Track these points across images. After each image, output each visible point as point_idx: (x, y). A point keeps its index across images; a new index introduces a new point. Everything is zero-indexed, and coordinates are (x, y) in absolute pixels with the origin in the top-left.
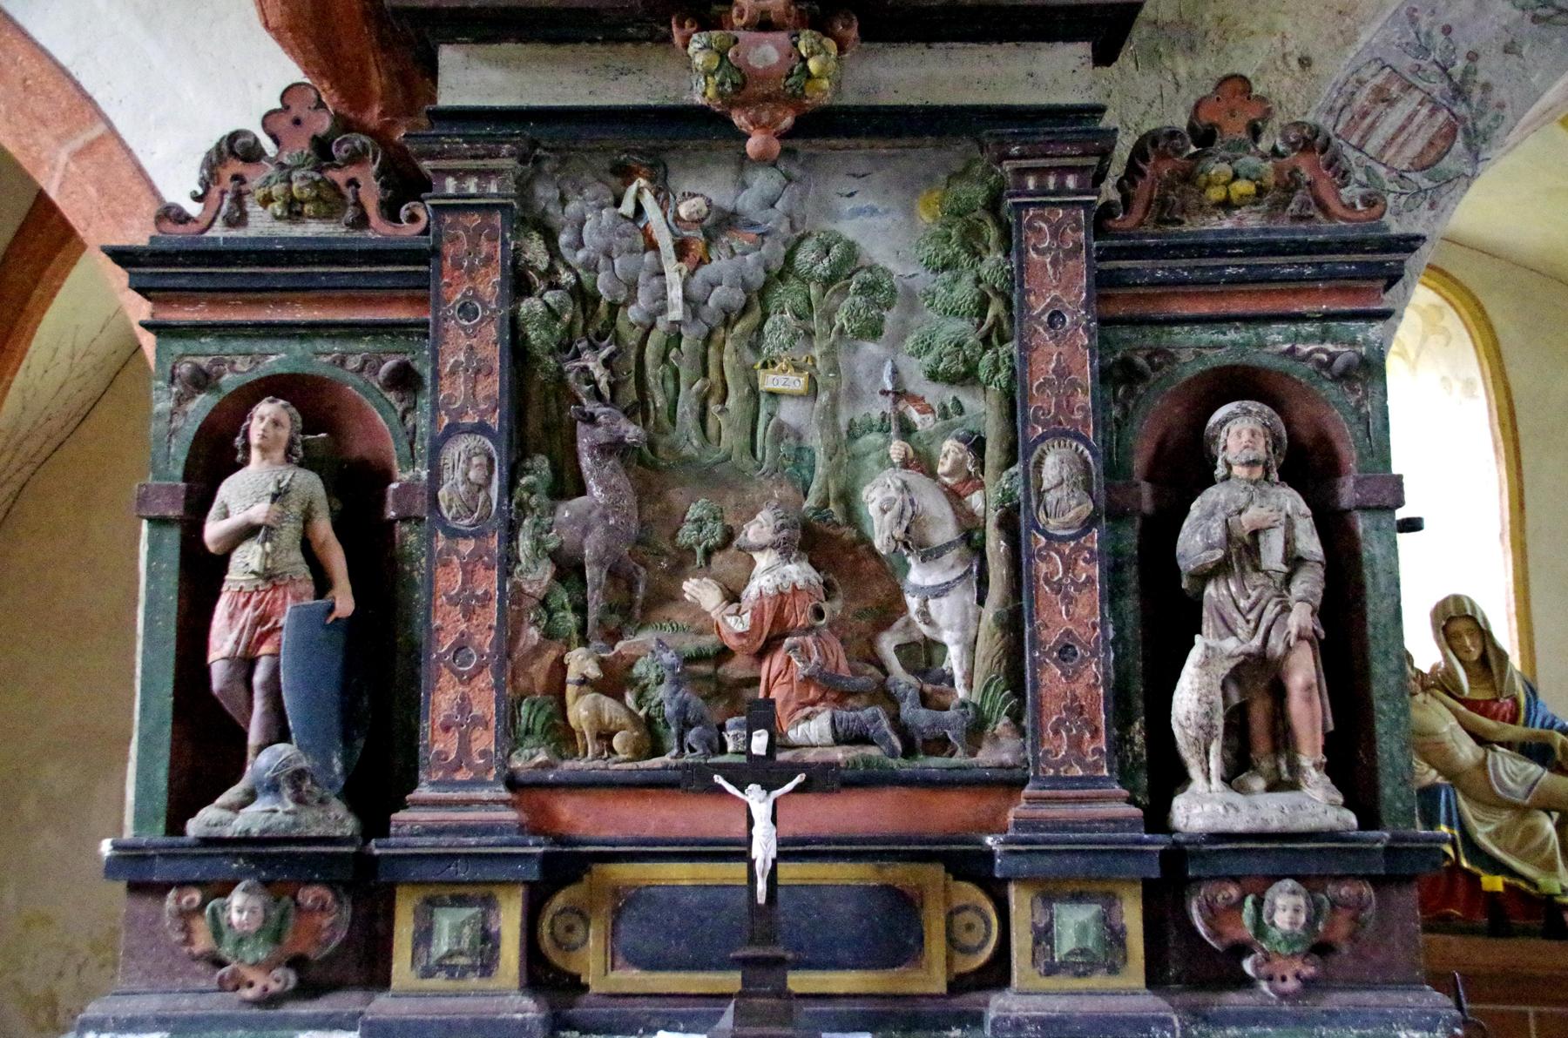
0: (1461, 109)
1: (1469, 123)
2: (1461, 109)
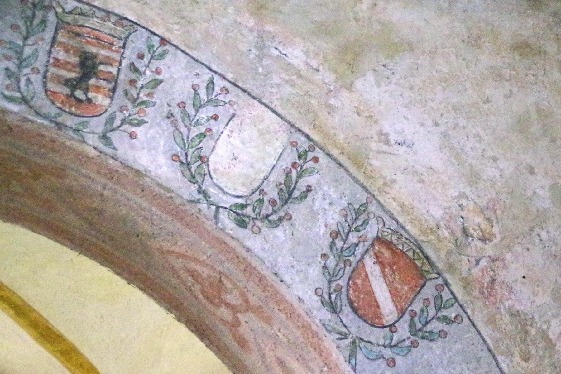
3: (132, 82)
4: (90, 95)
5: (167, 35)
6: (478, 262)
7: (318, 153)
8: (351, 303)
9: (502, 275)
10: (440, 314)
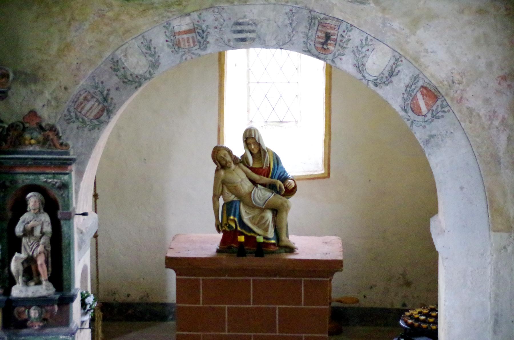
0: (106, 104)
1: (108, 108)
2: (106, 104)
3: (341, 41)
4: (328, 47)
5: (352, 23)
7: (403, 59)
9: (466, 95)
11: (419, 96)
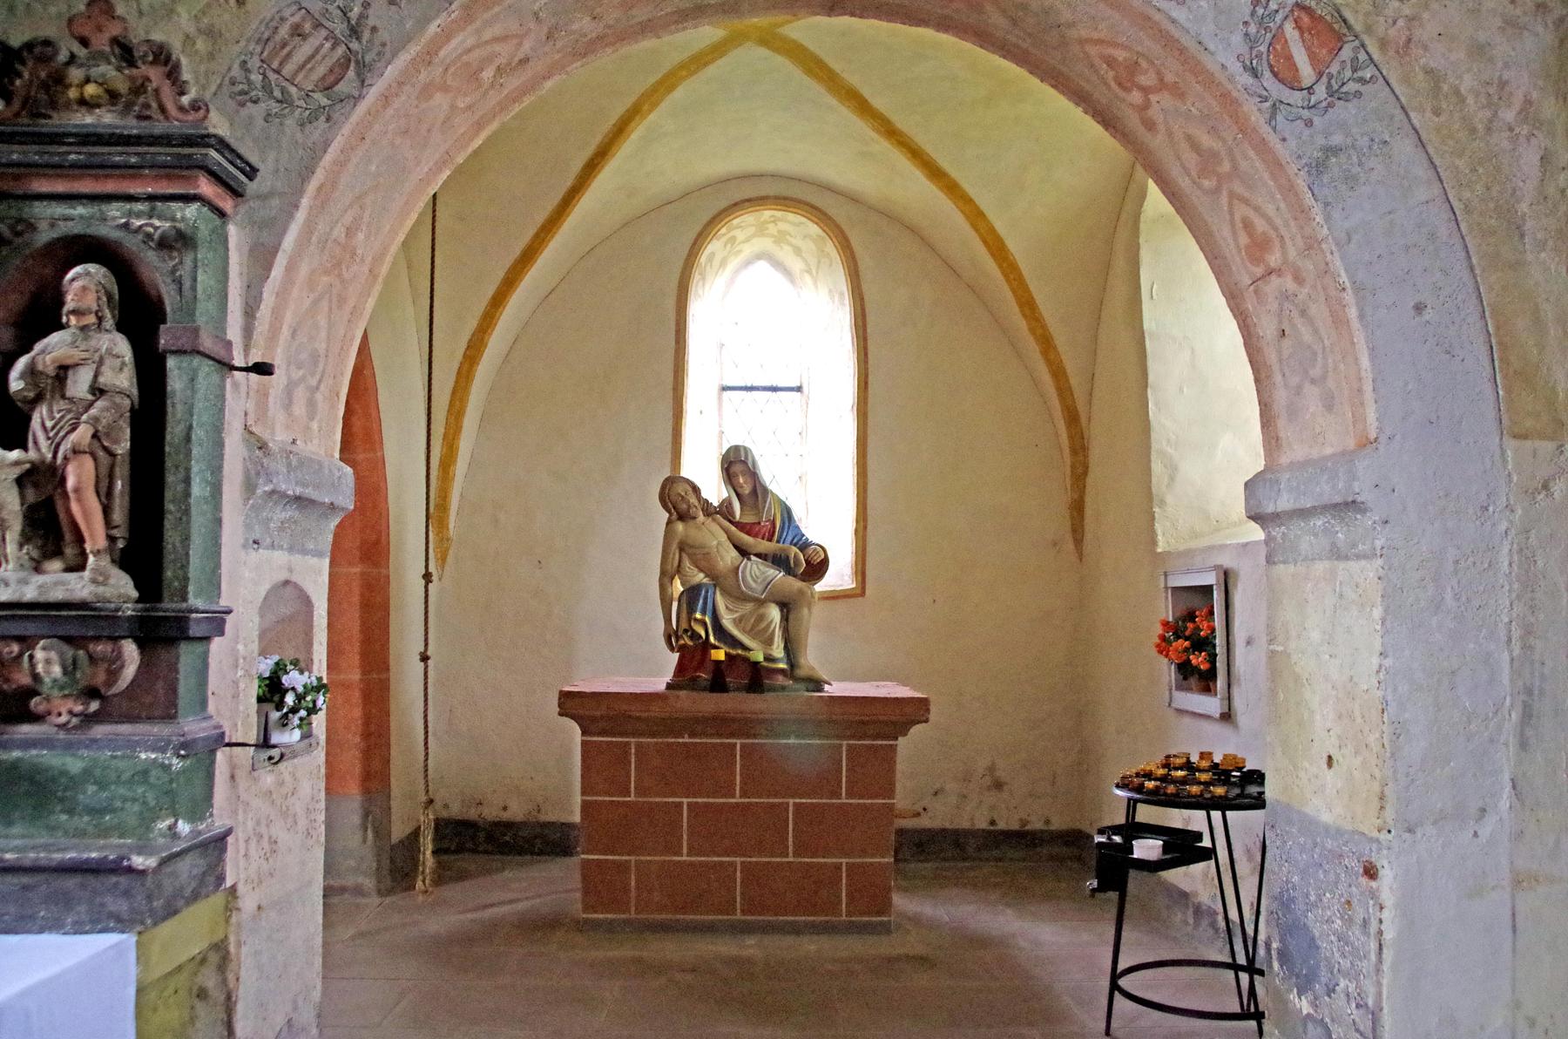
2: (355, 45)
6: (1395, 23)
8: (1271, 67)
10: (1355, 75)
11: (1290, 30)
